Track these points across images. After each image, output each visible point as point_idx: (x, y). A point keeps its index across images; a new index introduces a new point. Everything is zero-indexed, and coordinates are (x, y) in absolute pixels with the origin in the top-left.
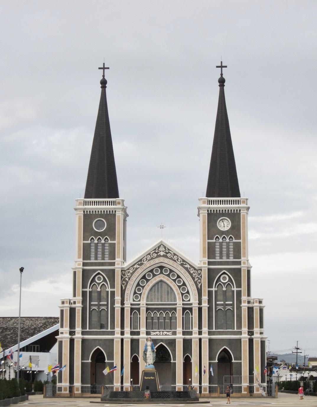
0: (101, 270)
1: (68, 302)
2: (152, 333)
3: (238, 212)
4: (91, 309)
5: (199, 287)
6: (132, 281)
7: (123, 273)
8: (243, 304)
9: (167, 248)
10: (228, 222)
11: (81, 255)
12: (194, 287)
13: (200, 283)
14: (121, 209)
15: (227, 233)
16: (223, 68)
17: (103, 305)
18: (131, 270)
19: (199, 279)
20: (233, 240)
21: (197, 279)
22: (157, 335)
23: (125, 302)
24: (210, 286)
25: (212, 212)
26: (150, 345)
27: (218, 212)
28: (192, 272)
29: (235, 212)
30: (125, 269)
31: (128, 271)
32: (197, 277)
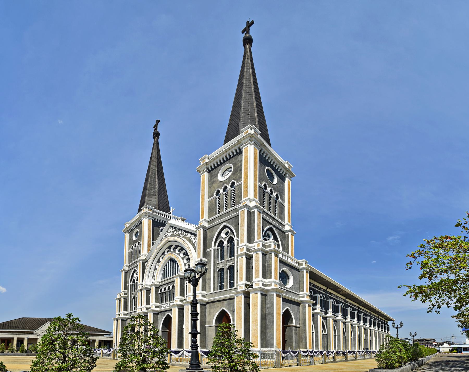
2: (163, 306)
9: (174, 227)
22: (166, 307)
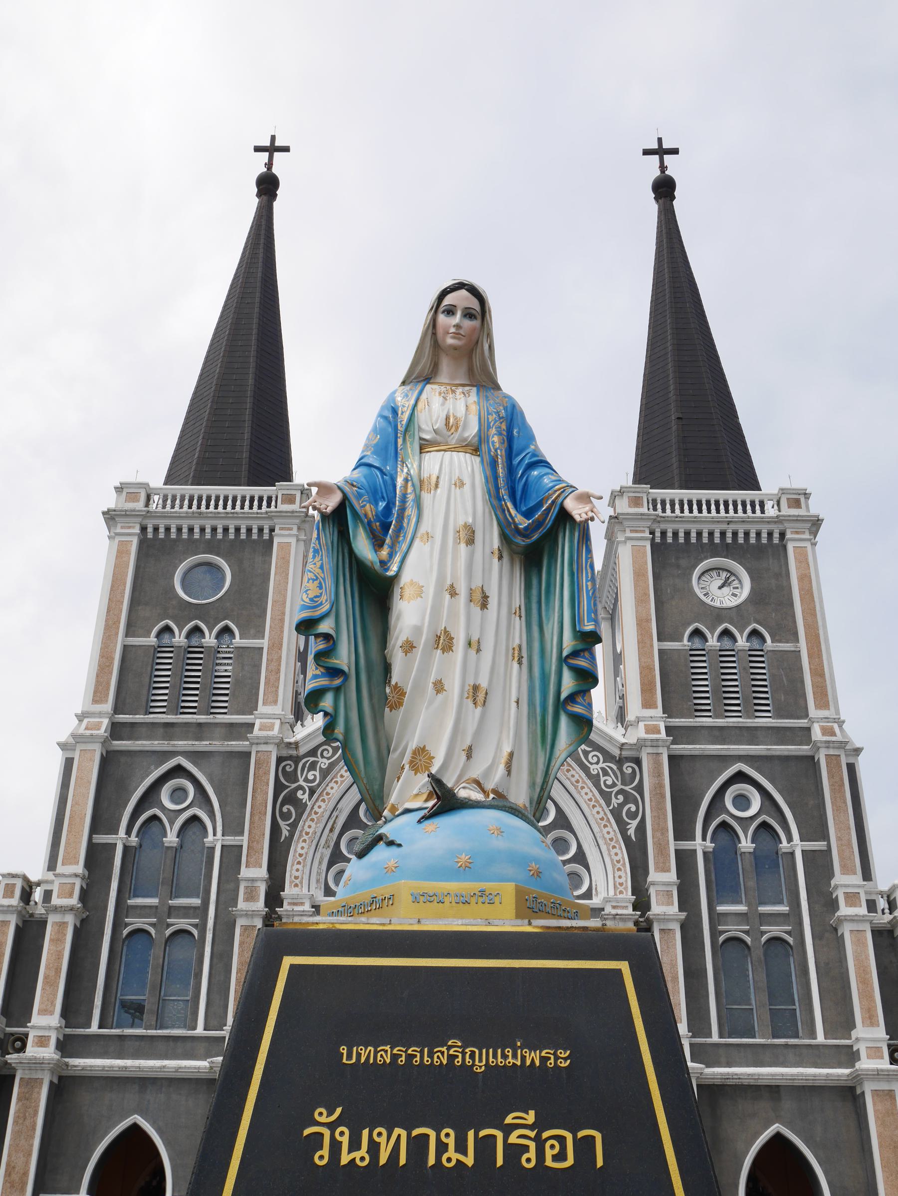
0: (194, 756)
1: (18, 893)
3: (776, 540)
4: (125, 932)
5: (631, 832)
6: (323, 801)
7: (288, 769)
8: (844, 910)
10: (736, 582)
11: (108, 689)
12: (609, 829)
13: (633, 815)
14: (297, 521)
15: (738, 614)
16: (665, 156)
17: (186, 911)
18: (322, 756)
19: (628, 798)
20: (763, 640)
21: (621, 798)
23: (288, 891)
24: (683, 831)
25: (670, 540)
26: (472, 430)
27: (693, 540)
28: (594, 769)
29: (764, 541)
30: (303, 750)
31: (312, 759)
32: (621, 792)
